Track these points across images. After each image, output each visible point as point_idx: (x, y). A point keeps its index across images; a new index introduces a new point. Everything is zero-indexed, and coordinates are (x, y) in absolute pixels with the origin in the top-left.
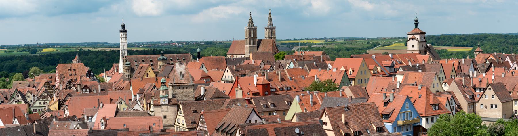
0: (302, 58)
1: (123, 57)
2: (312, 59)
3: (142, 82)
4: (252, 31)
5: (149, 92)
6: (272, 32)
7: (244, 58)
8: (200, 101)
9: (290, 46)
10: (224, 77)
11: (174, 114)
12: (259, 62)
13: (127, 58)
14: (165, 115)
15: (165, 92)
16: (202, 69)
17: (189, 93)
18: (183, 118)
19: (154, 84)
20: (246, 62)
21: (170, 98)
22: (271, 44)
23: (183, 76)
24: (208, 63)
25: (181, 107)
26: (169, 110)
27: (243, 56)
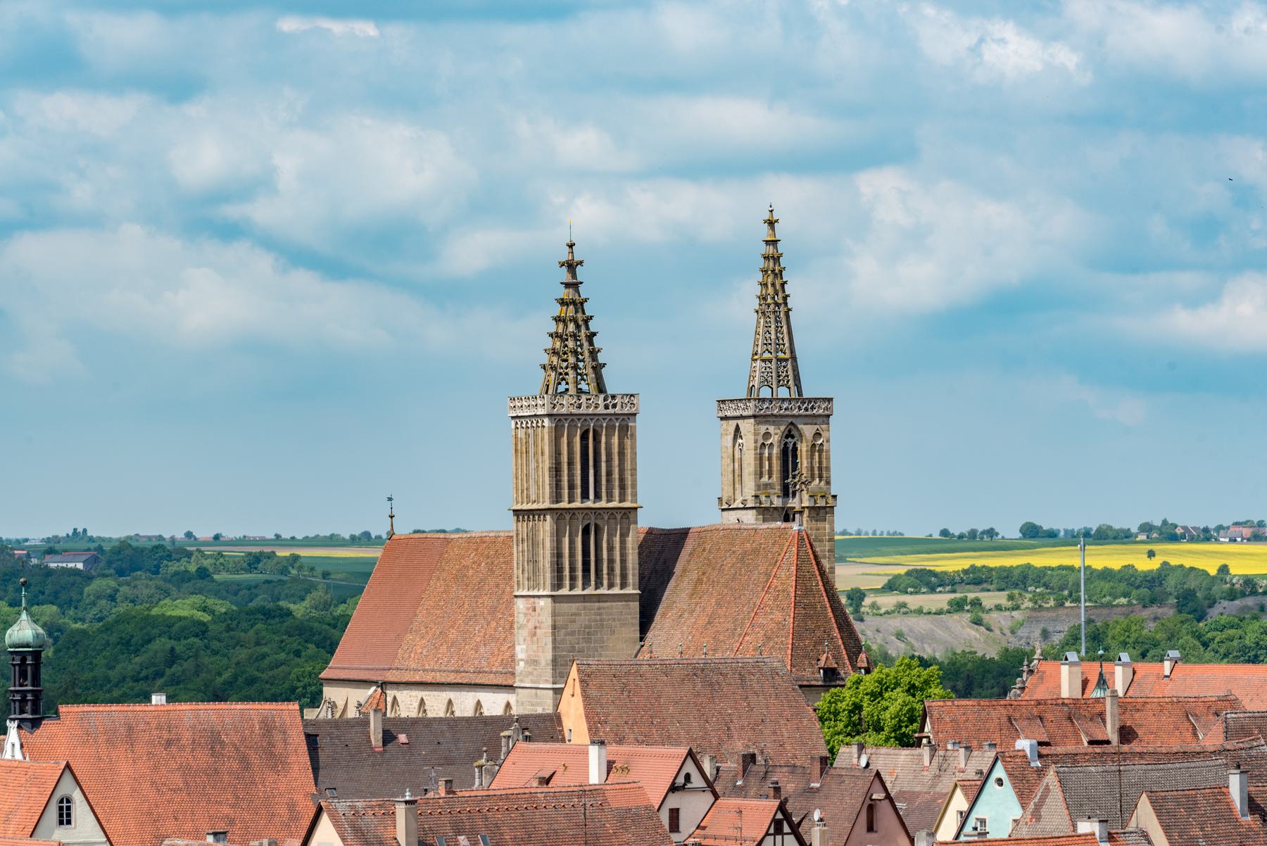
0: (1110, 732)
2: (1212, 737)
4: (589, 444)
6: (788, 456)
7: (503, 721)
9: (991, 599)
12: (654, 768)
16: (61, 834)
20: (520, 768)
22: (786, 577)
24: (125, 769)
27: (493, 704)
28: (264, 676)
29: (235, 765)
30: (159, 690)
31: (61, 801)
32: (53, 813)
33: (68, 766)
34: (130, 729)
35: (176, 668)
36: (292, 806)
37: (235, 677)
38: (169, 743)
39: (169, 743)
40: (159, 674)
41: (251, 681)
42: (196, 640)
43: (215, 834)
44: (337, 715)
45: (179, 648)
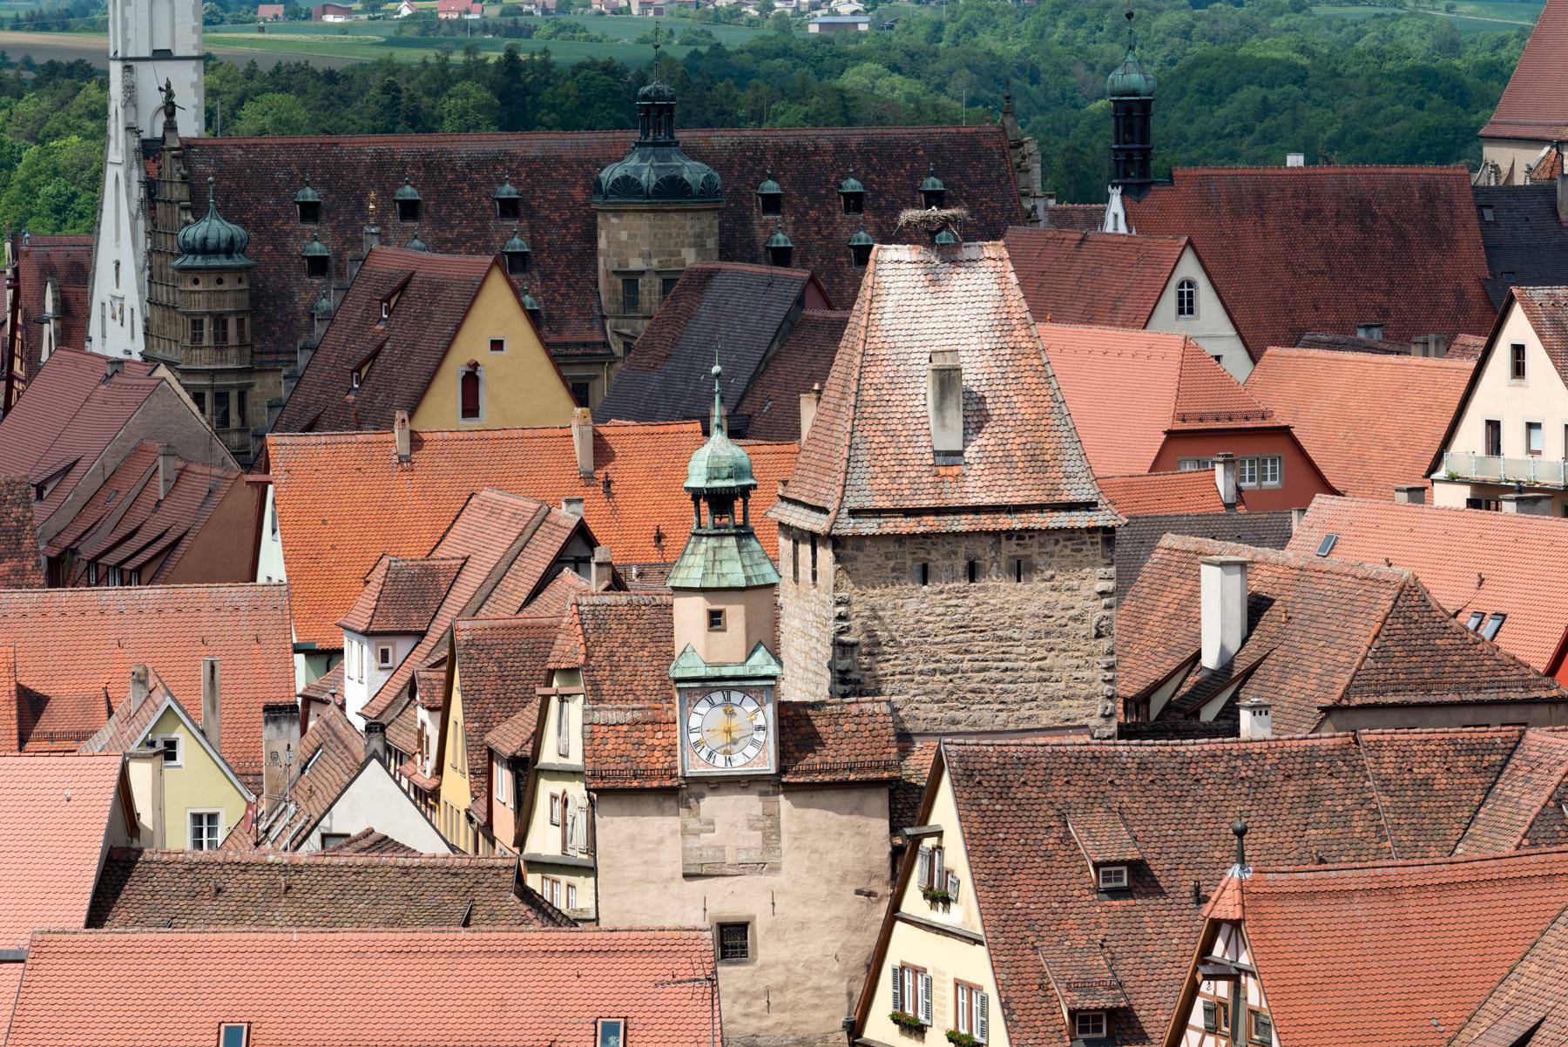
1: (149, 150)
3: (404, 487)
5: (505, 606)
8: (1191, 747)
10: (1471, 437)
11: (850, 904)
13: (206, 169)
14: (732, 910)
15: (735, 614)
16: (1186, 326)
17: (1051, 631)
18: (976, 965)
19: (567, 516)
21: (795, 690)
23: (976, 416)
25: (945, 811)
26: (789, 856)
28: (1378, 132)
29: (1390, 244)
30: (1297, 151)
31: (1181, 286)
32: (1170, 300)
33: (1190, 243)
34: (1260, 197)
35: (1268, 123)
36: (1460, 294)
37: (1343, 133)
38: (1308, 215)
39: (1308, 215)
40: (1247, 130)
41: (1364, 139)
42: (1295, 88)
43: (1368, 327)
44: (1502, 182)
45: (1273, 96)
